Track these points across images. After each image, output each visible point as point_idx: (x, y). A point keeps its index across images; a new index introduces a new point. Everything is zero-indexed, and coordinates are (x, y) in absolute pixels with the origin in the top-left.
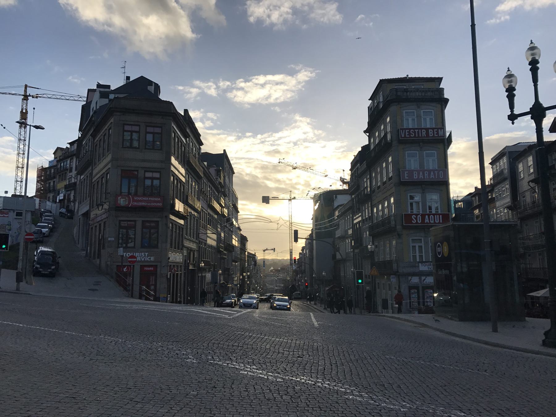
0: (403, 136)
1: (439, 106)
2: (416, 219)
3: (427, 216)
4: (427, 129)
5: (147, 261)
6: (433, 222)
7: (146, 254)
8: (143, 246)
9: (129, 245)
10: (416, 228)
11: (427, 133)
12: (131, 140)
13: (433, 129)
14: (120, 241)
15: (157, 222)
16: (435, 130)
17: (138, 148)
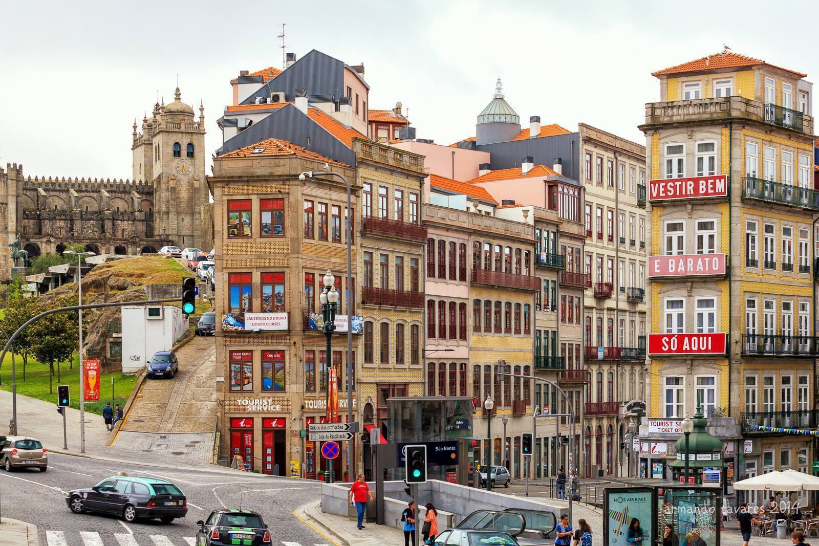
0: (655, 195)
1: (726, 131)
2: (669, 343)
3: (686, 340)
4: (696, 181)
5: (272, 413)
6: (696, 349)
7: (270, 401)
8: (264, 389)
9: (245, 388)
10: (669, 359)
11: (696, 189)
12: (241, 224)
13: (706, 179)
14: (233, 382)
15: (282, 352)
16: (710, 181)
17: (251, 237)
